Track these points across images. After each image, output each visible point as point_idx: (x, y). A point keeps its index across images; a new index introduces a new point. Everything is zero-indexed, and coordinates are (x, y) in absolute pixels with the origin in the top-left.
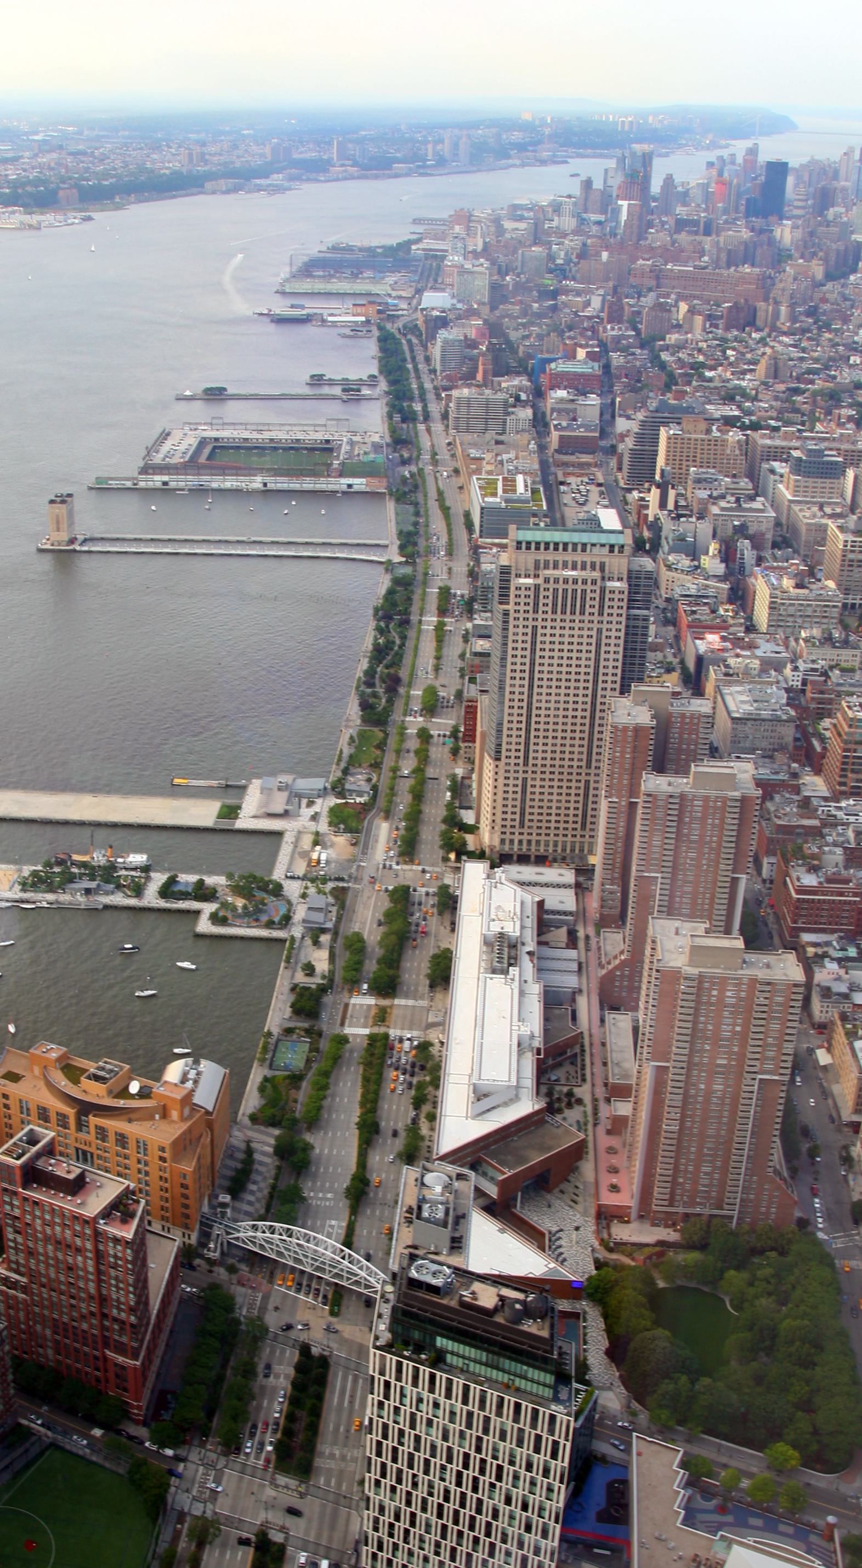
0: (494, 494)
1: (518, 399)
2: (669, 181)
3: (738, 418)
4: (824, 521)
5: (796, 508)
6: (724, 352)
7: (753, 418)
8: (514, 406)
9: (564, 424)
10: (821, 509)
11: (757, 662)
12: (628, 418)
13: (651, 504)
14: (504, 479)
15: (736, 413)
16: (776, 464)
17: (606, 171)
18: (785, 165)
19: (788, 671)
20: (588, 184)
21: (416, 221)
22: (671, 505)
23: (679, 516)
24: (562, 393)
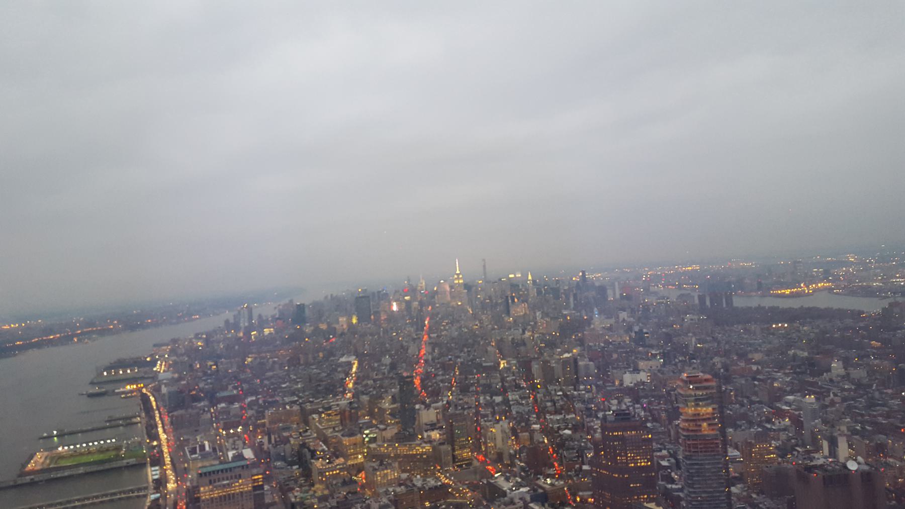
0: (195, 453)
1: (204, 411)
2: (260, 316)
3: (297, 401)
4: (336, 434)
5: (324, 431)
6: (289, 376)
7: (303, 399)
8: (202, 414)
9: (225, 417)
10: (334, 428)
11: (316, 500)
12: (252, 409)
13: (265, 443)
14: (200, 446)
15: (296, 399)
16: (314, 416)
17: (234, 316)
18: (303, 305)
19: (329, 500)
20: (227, 322)
21: (155, 345)
22: (273, 441)
23: (277, 445)
24: (223, 405)
